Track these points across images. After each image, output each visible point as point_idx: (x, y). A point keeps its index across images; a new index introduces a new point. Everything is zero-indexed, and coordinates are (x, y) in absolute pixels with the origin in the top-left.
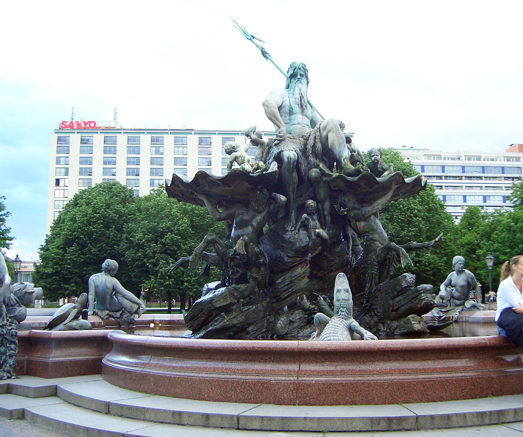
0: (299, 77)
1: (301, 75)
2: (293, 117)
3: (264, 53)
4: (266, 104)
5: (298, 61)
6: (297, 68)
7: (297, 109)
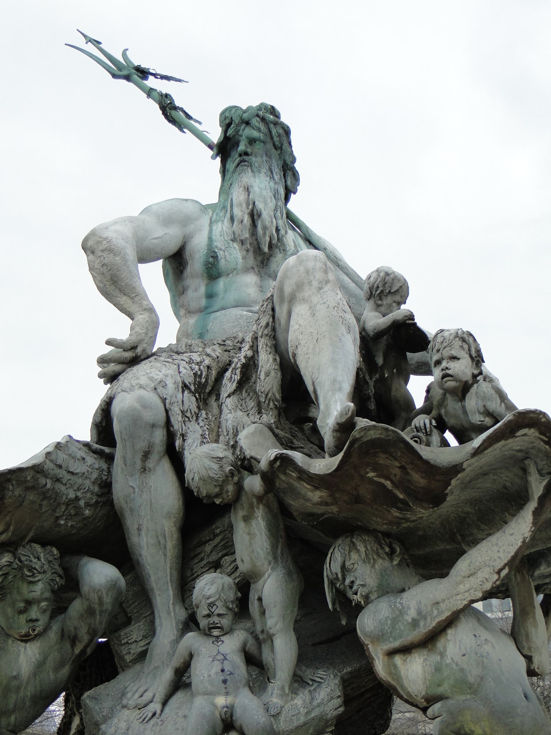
0: (242, 147)
1: (252, 141)
2: (221, 284)
3: (169, 109)
4: (90, 243)
5: (247, 100)
6: (236, 120)
7: (233, 255)
